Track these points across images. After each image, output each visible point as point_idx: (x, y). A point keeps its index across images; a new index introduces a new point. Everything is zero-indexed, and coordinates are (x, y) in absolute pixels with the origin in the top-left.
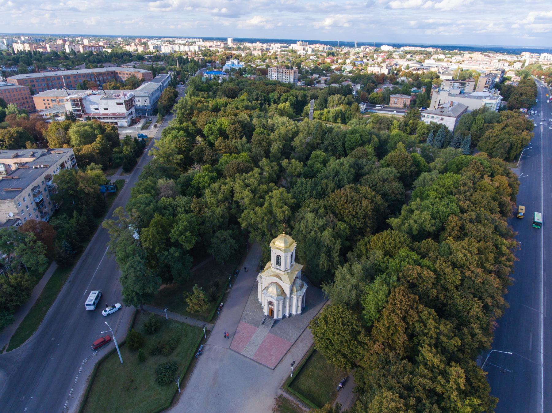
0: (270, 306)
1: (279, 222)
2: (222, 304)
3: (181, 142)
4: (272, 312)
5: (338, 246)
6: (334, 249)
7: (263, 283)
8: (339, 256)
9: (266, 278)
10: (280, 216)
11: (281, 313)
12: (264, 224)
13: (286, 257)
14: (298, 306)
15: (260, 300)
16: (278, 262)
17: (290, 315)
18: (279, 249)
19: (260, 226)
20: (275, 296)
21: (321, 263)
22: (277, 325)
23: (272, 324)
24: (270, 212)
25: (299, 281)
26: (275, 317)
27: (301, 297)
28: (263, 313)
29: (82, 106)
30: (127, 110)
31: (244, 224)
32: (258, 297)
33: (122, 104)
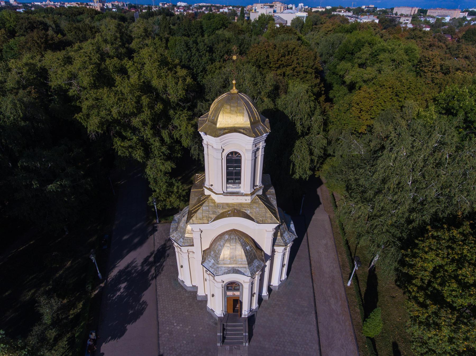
0: (230, 293)
2: (93, 336)
4: (234, 304)
5: (317, 119)
7: (197, 242)
9: (203, 227)
10: (175, 92)
11: (255, 299)
12: (143, 116)
13: (255, 152)
14: (283, 266)
15: (188, 284)
19: (135, 122)
24: (146, 88)
26: (245, 312)
27: (290, 245)
28: (210, 314)
31: (92, 125)
32: (180, 277)
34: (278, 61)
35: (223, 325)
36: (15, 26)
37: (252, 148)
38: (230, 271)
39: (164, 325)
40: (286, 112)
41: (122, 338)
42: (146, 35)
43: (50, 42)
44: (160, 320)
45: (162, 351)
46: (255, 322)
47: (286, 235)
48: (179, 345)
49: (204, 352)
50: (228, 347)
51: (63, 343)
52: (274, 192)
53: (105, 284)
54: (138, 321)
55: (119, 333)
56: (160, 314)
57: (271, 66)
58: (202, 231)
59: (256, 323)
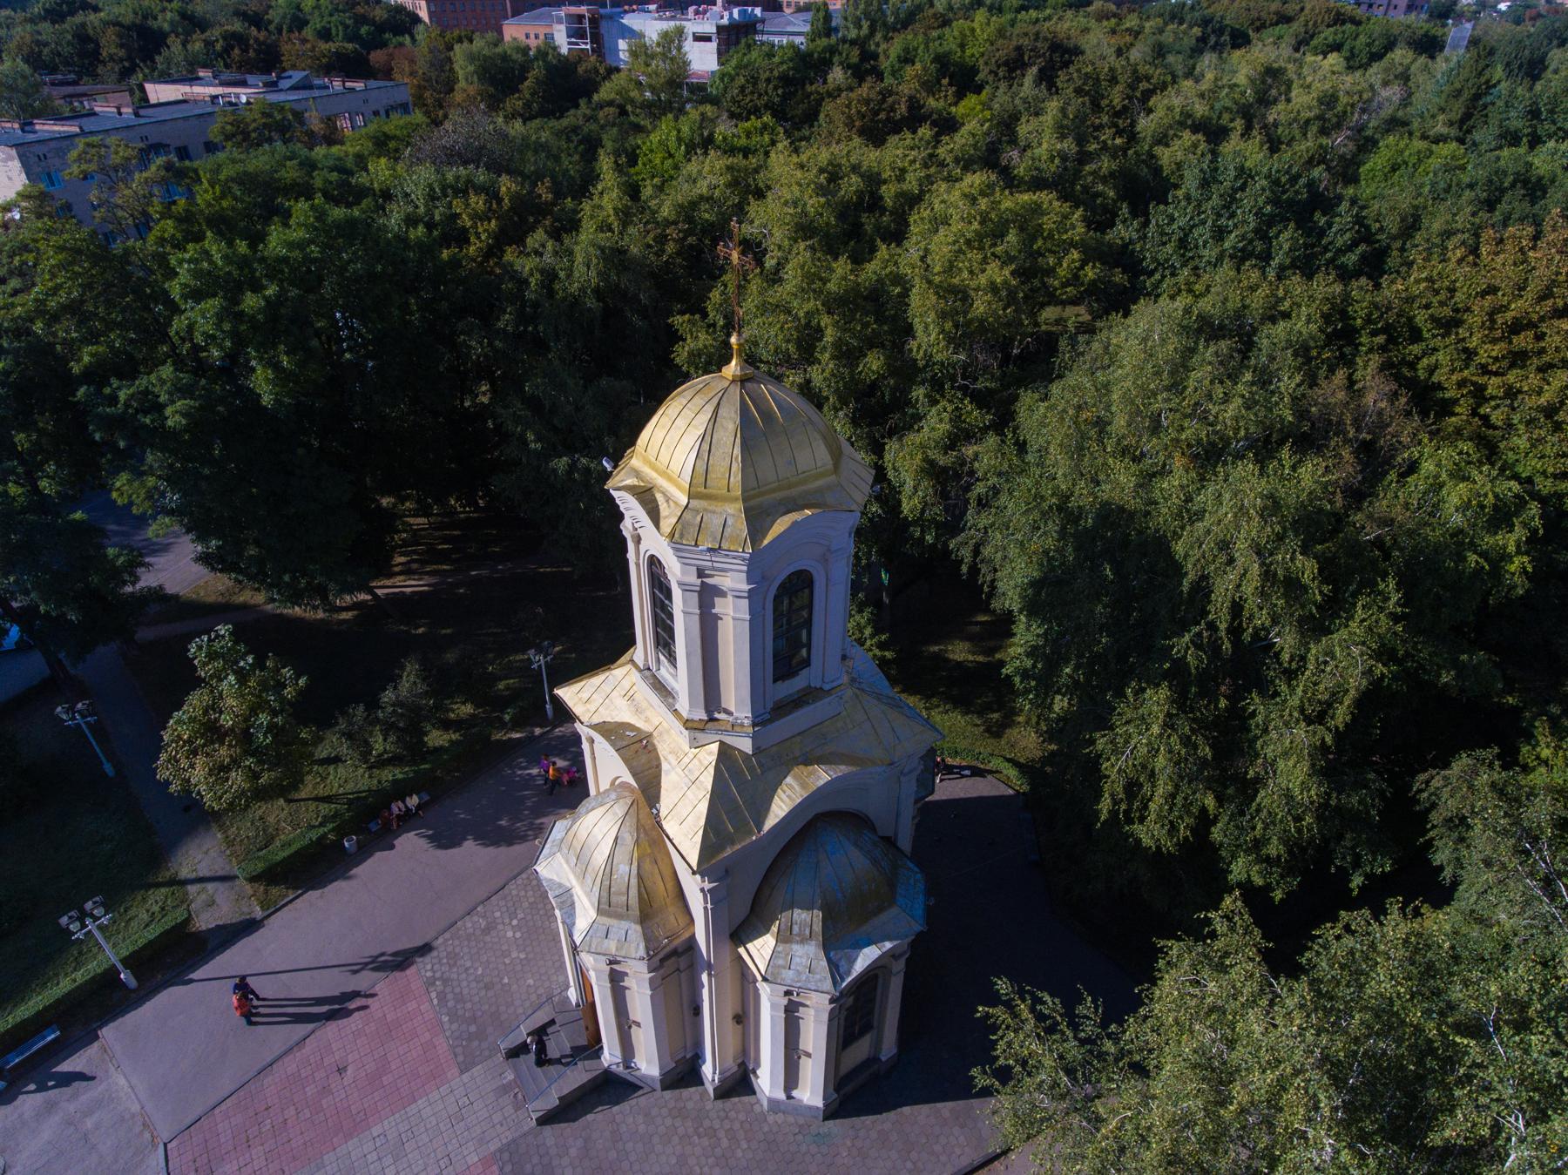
1: (937, 386)
2: (413, 801)
3: (762, 86)
6: (1290, 675)
8: (1333, 765)
13: (707, 595)
16: (664, 639)
17: (739, 1083)
18: (646, 496)
20: (585, 915)
21: (1115, 770)
22: (598, 1120)
23: (551, 1101)
25: (847, 861)
26: (610, 1055)
29: (597, 39)
30: (720, 63)
33: (707, 39)
34: (1516, 328)
35: (552, 1022)
36: (982, 55)
37: (683, 573)
38: (560, 885)
39: (502, 903)
40: (1179, 548)
41: (440, 853)
42: (1320, 118)
43: (882, 116)
44: (512, 886)
45: (435, 944)
46: (618, 1103)
47: (808, 955)
48: (468, 964)
49: (473, 1028)
50: (510, 1076)
51: (389, 775)
52: (821, 783)
53: (542, 735)
54: (491, 849)
55: (445, 839)
56: (524, 876)
57: (1473, 343)
58: (592, 741)
59: (616, 1109)
